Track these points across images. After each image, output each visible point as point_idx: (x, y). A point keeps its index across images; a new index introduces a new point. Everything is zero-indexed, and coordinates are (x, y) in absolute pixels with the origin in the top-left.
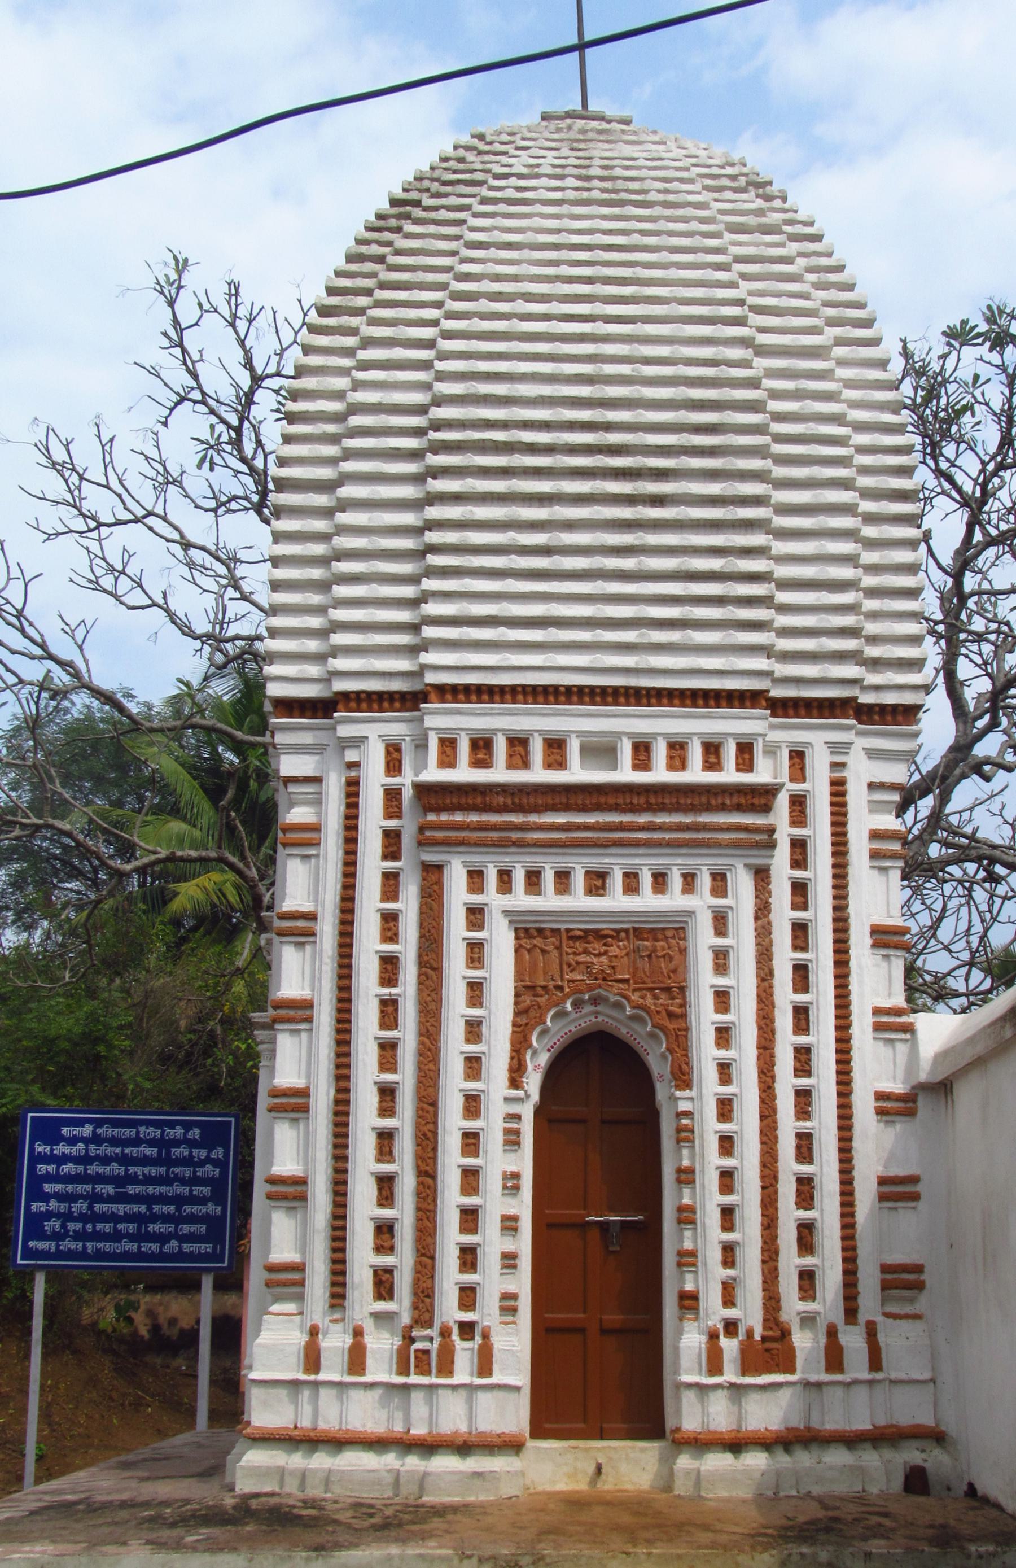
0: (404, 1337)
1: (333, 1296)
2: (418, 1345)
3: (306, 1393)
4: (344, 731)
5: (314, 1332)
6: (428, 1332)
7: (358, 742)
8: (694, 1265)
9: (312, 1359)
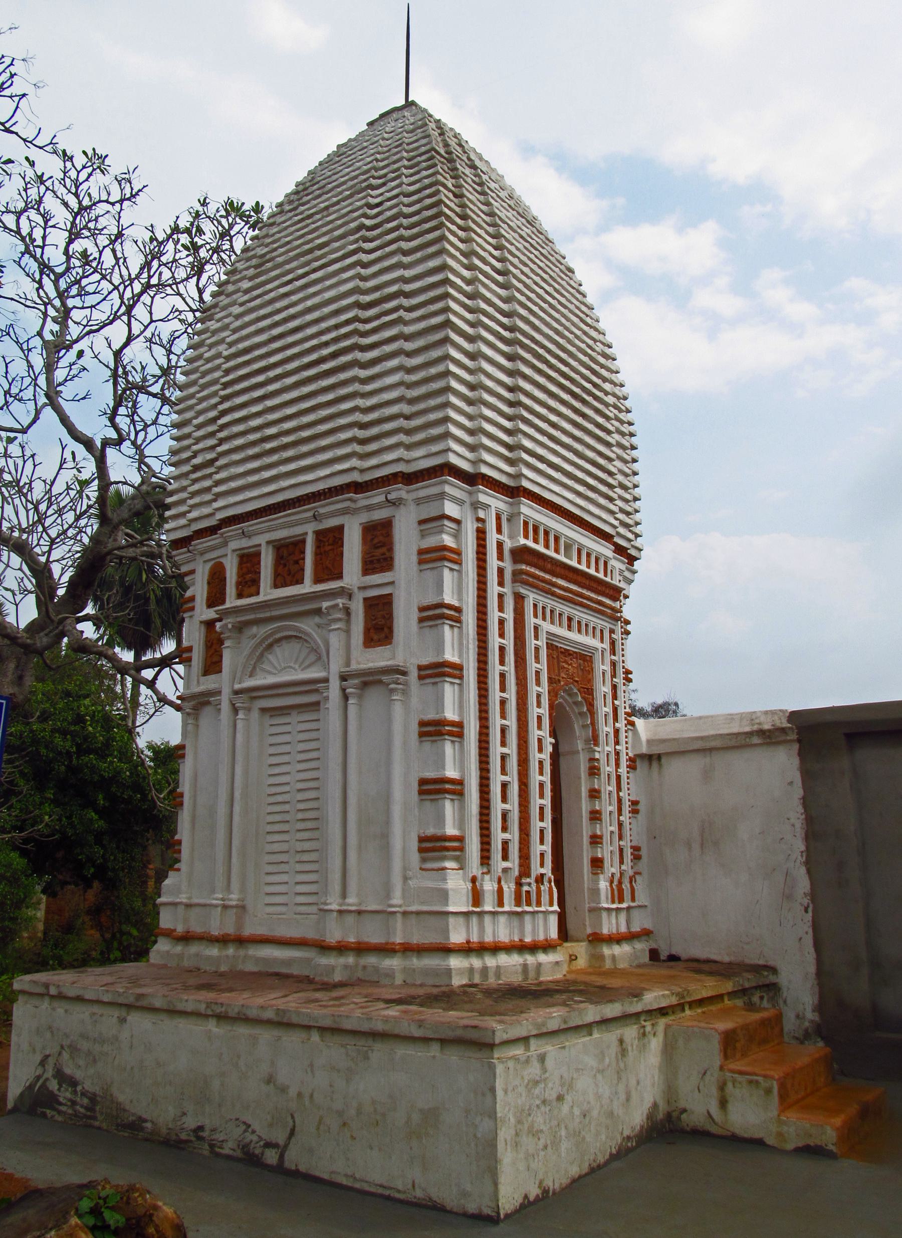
0: (516, 883)
1: (482, 857)
2: (525, 888)
3: (474, 920)
4: (482, 498)
5: (474, 880)
6: (528, 880)
7: (487, 507)
8: (601, 843)
9: (477, 897)
